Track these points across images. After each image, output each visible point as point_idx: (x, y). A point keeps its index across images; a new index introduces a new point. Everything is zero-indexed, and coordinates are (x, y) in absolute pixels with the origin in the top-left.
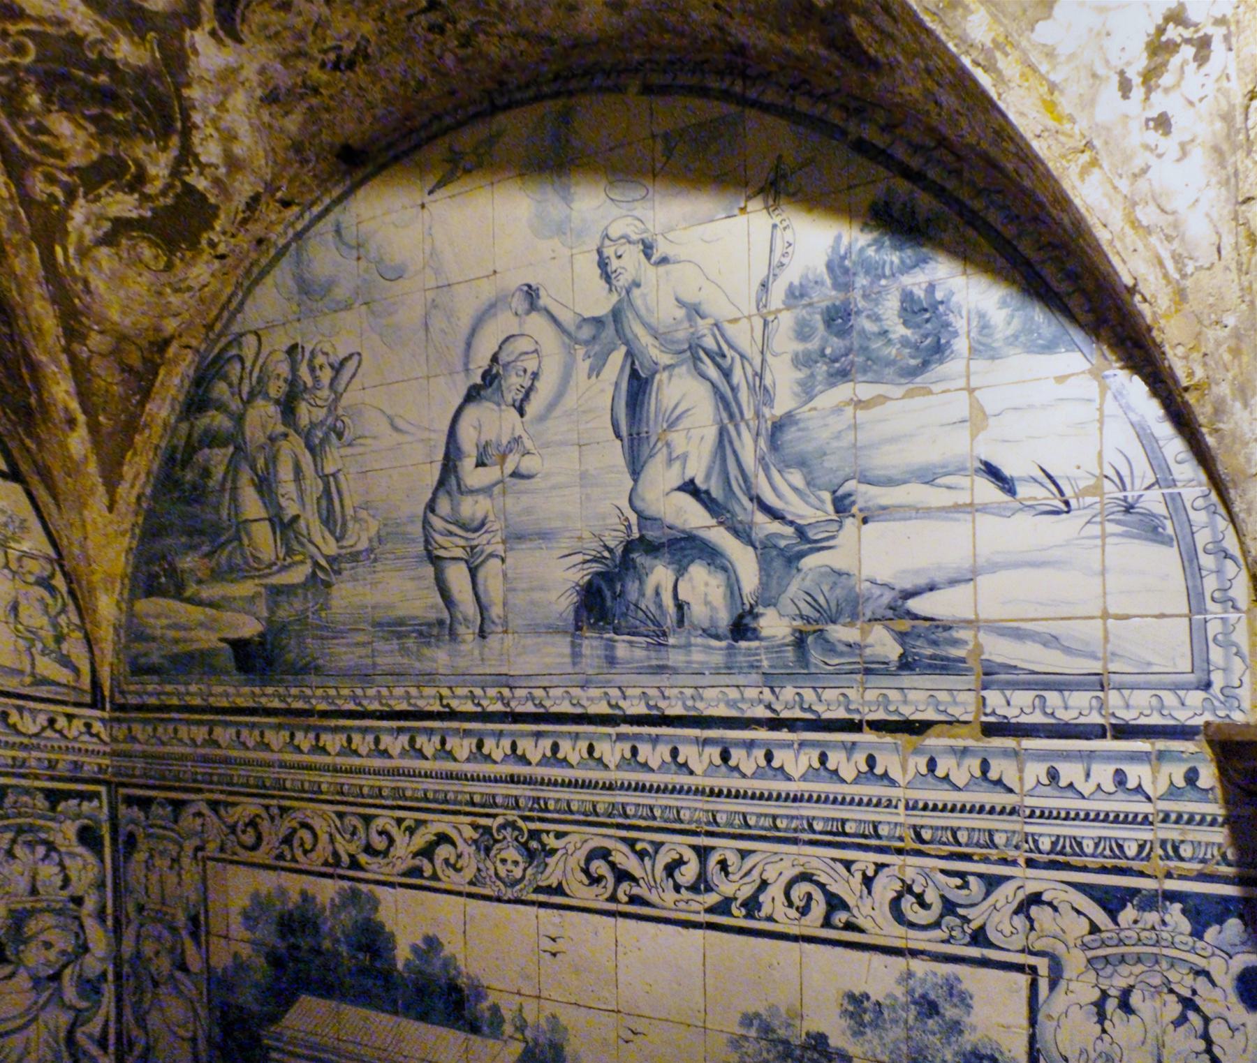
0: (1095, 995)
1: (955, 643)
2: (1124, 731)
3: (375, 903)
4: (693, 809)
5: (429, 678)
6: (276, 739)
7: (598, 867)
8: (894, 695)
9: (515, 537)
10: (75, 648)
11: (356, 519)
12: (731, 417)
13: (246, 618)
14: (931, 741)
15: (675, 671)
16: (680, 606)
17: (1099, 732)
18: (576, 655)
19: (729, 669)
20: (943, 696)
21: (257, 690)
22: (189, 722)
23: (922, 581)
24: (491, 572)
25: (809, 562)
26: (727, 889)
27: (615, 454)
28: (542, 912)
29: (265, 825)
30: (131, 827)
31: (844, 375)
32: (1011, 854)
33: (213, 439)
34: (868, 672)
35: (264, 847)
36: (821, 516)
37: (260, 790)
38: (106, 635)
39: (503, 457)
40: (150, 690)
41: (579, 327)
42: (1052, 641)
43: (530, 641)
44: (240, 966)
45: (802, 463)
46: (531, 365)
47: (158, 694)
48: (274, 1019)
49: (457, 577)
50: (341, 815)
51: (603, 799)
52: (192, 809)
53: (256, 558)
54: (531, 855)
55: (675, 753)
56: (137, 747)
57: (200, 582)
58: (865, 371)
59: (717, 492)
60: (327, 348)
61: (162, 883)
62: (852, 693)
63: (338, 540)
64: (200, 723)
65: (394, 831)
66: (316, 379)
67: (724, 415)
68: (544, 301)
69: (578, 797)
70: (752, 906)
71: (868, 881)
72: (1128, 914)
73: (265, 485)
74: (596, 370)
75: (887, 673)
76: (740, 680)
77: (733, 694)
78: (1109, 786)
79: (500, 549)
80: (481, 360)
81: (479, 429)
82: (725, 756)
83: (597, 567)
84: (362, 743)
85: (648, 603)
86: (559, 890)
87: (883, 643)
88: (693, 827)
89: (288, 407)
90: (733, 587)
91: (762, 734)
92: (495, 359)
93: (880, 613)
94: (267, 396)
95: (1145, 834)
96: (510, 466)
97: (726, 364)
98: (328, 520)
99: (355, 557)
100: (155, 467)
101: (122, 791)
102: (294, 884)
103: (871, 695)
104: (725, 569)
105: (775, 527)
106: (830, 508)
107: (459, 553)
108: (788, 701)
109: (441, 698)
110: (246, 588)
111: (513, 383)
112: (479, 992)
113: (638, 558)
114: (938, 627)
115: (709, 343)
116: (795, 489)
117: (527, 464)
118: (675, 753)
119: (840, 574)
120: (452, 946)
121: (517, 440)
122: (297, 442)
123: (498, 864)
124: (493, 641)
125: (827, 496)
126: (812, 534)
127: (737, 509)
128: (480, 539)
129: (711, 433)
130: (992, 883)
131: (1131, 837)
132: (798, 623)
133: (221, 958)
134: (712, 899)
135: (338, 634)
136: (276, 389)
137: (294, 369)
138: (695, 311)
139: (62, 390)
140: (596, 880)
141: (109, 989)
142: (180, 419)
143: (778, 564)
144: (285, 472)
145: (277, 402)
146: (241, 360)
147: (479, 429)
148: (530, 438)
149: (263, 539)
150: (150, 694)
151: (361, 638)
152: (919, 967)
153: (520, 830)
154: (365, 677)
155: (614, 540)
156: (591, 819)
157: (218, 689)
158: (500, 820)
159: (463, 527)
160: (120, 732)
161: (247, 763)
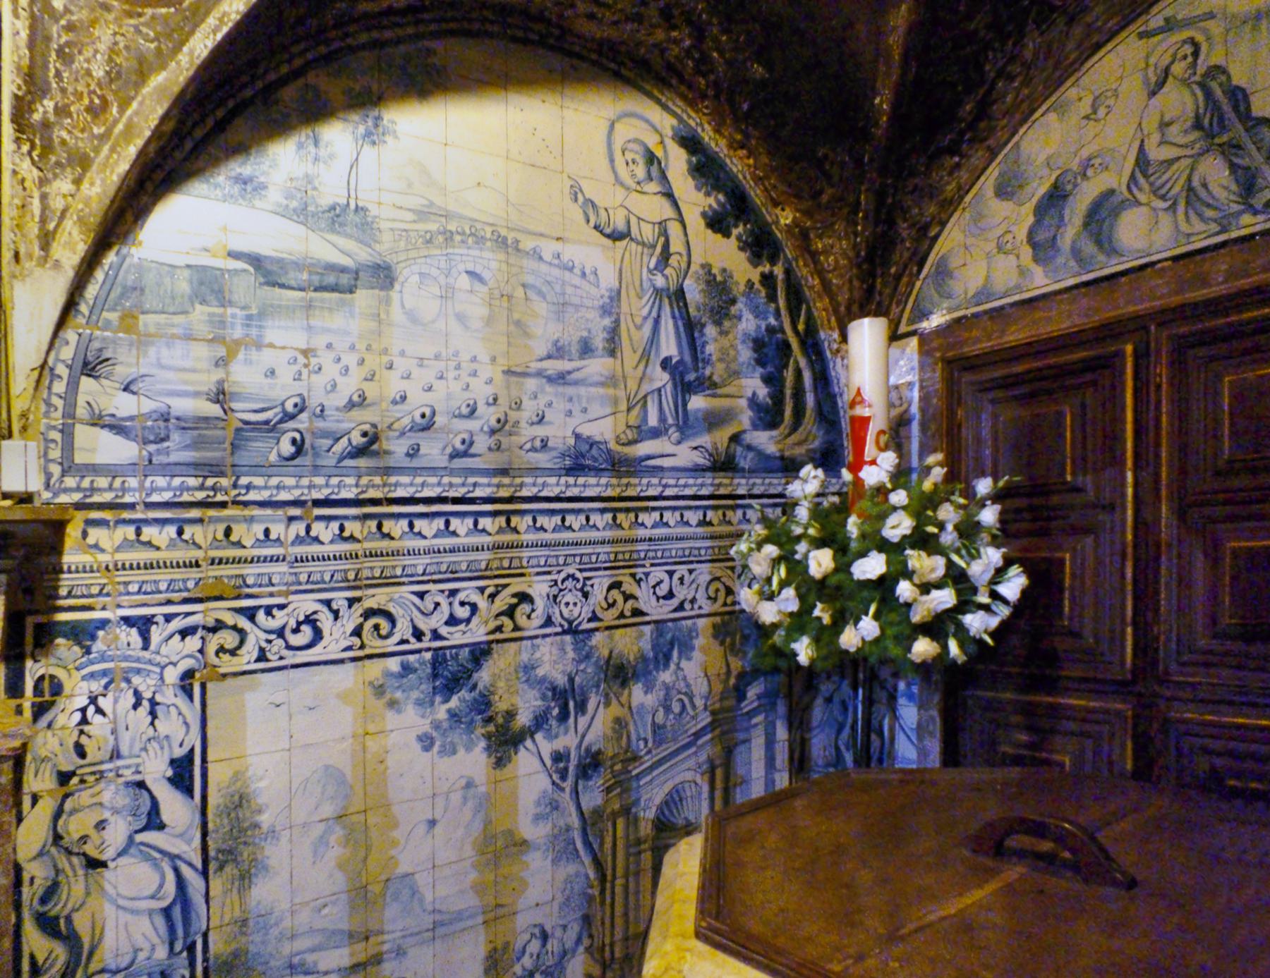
50: (421, 595)
65: (475, 598)
123: (563, 606)
134: (675, 602)
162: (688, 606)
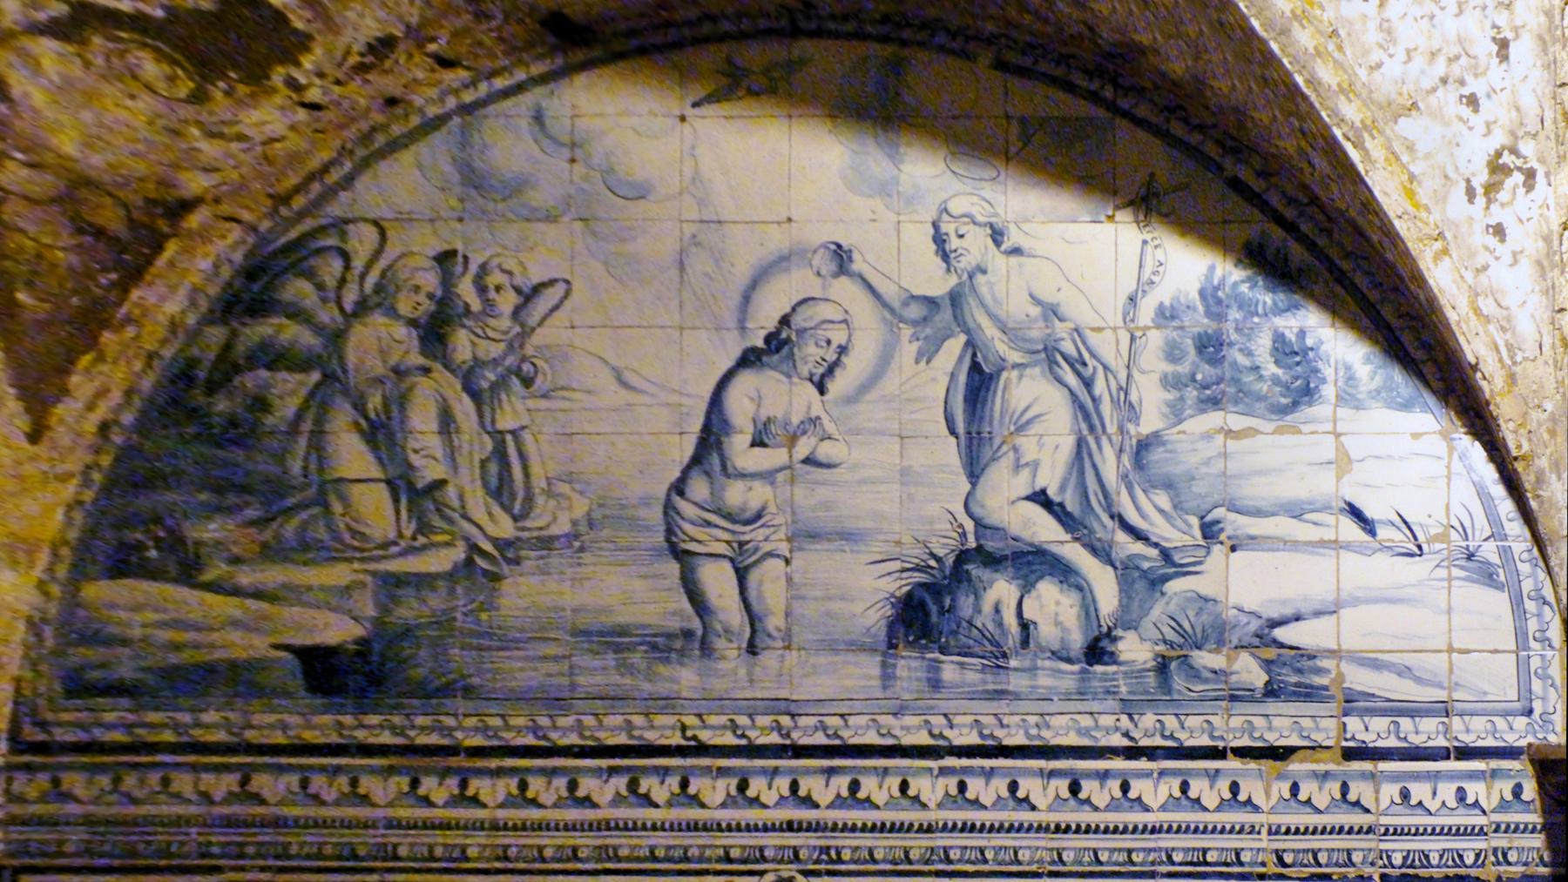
1: (1319, 671)
8: (1259, 722)
12: (1092, 428)
14: (1295, 766)
15: (1016, 696)
16: (1025, 626)
19: (1082, 694)
20: (1306, 723)
23: (1288, 611)
25: (1173, 586)
27: (949, 453)
34: (1233, 698)
36: (1188, 540)
45: (1169, 485)
59: (1072, 505)
62: (1215, 720)
67: (1084, 426)
75: (1253, 700)
76: (1095, 706)
77: (1086, 721)
82: (1075, 789)
85: (985, 620)
87: (1248, 670)
90: (1089, 608)
91: (1119, 764)
93: (1247, 640)
97: (1087, 372)
103: (1236, 722)
104: (1079, 588)
105: (1138, 548)
106: (1197, 533)
113: (974, 569)
115: (1068, 347)
116: (1161, 511)
119: (1206, 600)
125: (1195, 521)
126: (1177, 558)
127: (1096, 525)
129: (1068, 443)
132: (1161, 648)
138: (1052, 312)
143: (1140, 586)
155: (944, 547)
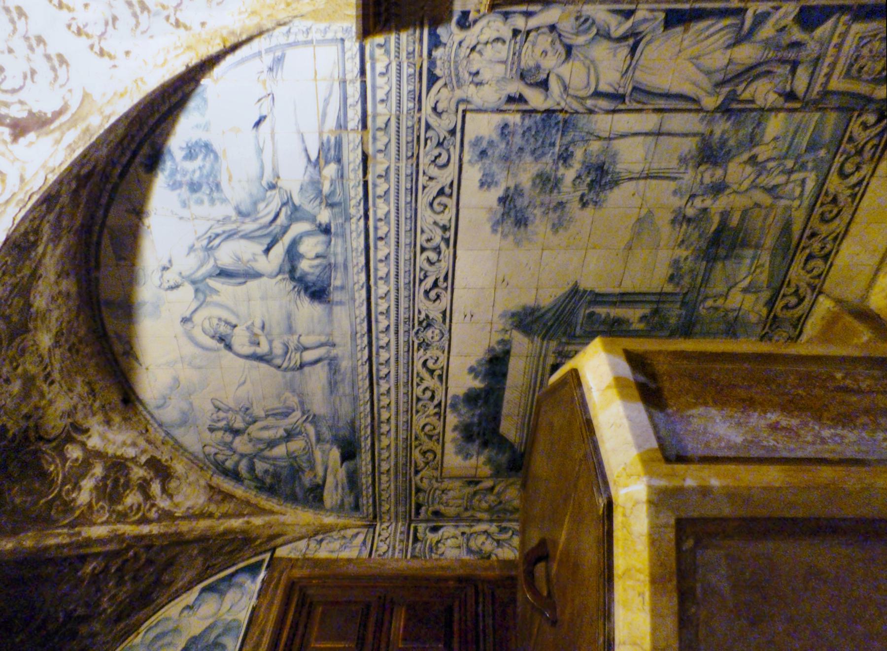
0: (472, 87)
1: (329, 141)
2: (363, 72)
3: (455, 397)
4: (405, 254)
5: (354, 369)
6: (385, 441)
7: (432, 294)
8: (351, 167)
9: (290, 330)
10: (349, 533)
11: (285, 402)
12: (235, 234)
13: (331, 455)
14: (370, 151)
15: (346, 260)
16: (317, 256)
17: (364, 83)
18: (341, 303)
19: (343, 235)
20: (351, 146)
21: (363, 451)
22: (380, 483)
23: (303, 154)
24: (306, 341)
25: (297, 200)
26: (437, 240)
27: (253, 284)
28: (454, 321)
29: (425, 448)
30: (429, 513)
31: (218, 186)
32: (416, 119)
33: (252, 468)
34: (342, 176)
35: (434, 448)
36: (277, 195)
37: (408, 449)
38: (342, 521)
39: (255, 335)
40: (366, 501)
41: (198, 300)
42: (327, 102)
43: (336, 325)
44: (489, 461)
45: (255, 204)
46: (215, 321)
47: (368, 498)
48: (512, 446)
49: (309, 356)
51: (403, 293)
52: (419, 482)
53: (304, 449)
54: (429, 325)
55: (381, 261)
56: (392, 509)
57: (315, 476)
58: (216, 176)
59: (268, 240)
60: (210, 413)
61: (454, 498)
62: (352, 184)
63: (294, 411)
64: (380, 479)
66: (223, 419)
67: (235, 236)
68: (187, 314)
69: (403, 304)
70: (445, 228)
71: (431, 179)
72: (438, 72)
73: (272, 444)
74: (217, 292)
75: (342, 168)
76: (348, 232)
77: (354, 235)
78: (385, 79)
79: (296, 337)
80: (213, 343)
81: (243, 345)
82: (381, 239)
83: (302, 293)
84: (385, 401)
85: (317, 271)
86: (444, 313)
87: (330, 170)
88: (412, 255)
89: (236, 432)
90: (308, 234)
91: (371, 223)
92: (213, 337)
93: (317, 172)
94: (232, 443)
95: (405, 65)
96: (259, 331)
97: (213, 236)
98: (286, 415)
99: (302, 403)
100: (264, 497)
101: (413, 518)
102: (450, 435)
103: (352, 176)
104: (301, 237)
105: (282, 216)
106: (274, 192)
107: (298, 355)
108: (356, 211)
109: (362, 365)
110: (318, 455)
111: (223, 329)
112: (491, 350)
113: (298, 274)
114: (323, 148)
115: (205, 242)
116: (266, 206)
117: (258, 324)
118: (381, 261)
119: (301, 189)
120: (472, 362)
121: (248, 328)
122: (252, 428)
124: (337, 340)
125: (269, 193)
126: (285, 200)
127: (275, 232)
128: (292, 346)
129: (244, 243)
130: (428, 127)
131: (406, 71)
132: (323, 206)
133: (486, 470)
134: (443, 246)
135: (336, 411)
136: (228, 437)
137: (219, 429)
138: (192, 249)
139: (236, 523)
140: (438, 297)
141: (504, 525)
142: (242, 484)
143: (298, 214)
144: (266, 434)
145: (234, 438)
146: (216, 454)
147: (243, 345)
148: (246, 322)
149: (296, 445)
150: (368, 502)
151: (338, 402)
152: (466, 157)
153: (418, 330)
154: (355, 399)
155: (290, 285)
156: (412, 298)
157: (364, 469)
158: (415, 339)
159: (286, 353)
160: (386, 517)
161: (396, 455)
162: (447, 235)
